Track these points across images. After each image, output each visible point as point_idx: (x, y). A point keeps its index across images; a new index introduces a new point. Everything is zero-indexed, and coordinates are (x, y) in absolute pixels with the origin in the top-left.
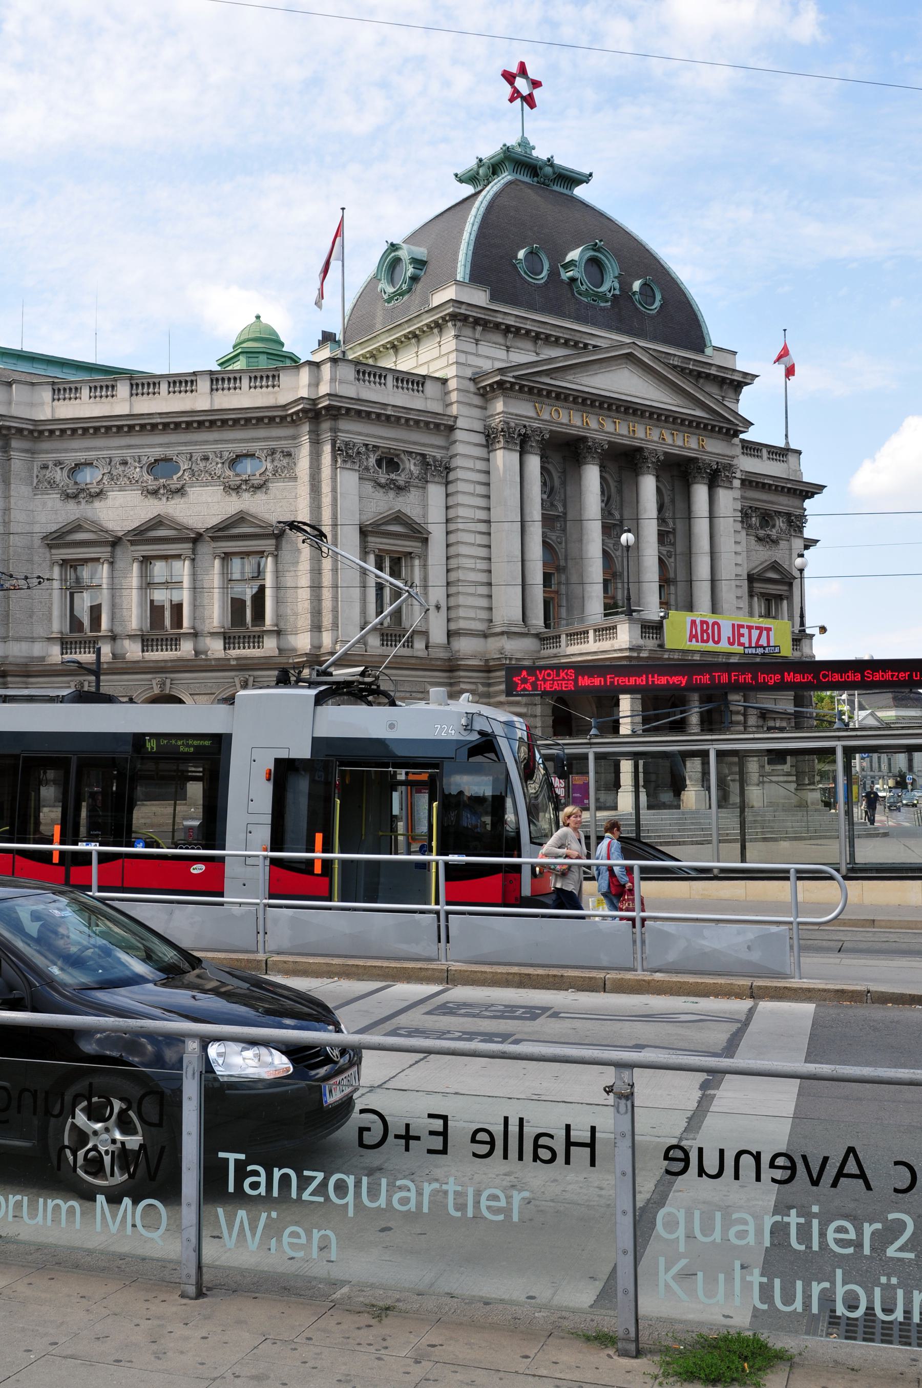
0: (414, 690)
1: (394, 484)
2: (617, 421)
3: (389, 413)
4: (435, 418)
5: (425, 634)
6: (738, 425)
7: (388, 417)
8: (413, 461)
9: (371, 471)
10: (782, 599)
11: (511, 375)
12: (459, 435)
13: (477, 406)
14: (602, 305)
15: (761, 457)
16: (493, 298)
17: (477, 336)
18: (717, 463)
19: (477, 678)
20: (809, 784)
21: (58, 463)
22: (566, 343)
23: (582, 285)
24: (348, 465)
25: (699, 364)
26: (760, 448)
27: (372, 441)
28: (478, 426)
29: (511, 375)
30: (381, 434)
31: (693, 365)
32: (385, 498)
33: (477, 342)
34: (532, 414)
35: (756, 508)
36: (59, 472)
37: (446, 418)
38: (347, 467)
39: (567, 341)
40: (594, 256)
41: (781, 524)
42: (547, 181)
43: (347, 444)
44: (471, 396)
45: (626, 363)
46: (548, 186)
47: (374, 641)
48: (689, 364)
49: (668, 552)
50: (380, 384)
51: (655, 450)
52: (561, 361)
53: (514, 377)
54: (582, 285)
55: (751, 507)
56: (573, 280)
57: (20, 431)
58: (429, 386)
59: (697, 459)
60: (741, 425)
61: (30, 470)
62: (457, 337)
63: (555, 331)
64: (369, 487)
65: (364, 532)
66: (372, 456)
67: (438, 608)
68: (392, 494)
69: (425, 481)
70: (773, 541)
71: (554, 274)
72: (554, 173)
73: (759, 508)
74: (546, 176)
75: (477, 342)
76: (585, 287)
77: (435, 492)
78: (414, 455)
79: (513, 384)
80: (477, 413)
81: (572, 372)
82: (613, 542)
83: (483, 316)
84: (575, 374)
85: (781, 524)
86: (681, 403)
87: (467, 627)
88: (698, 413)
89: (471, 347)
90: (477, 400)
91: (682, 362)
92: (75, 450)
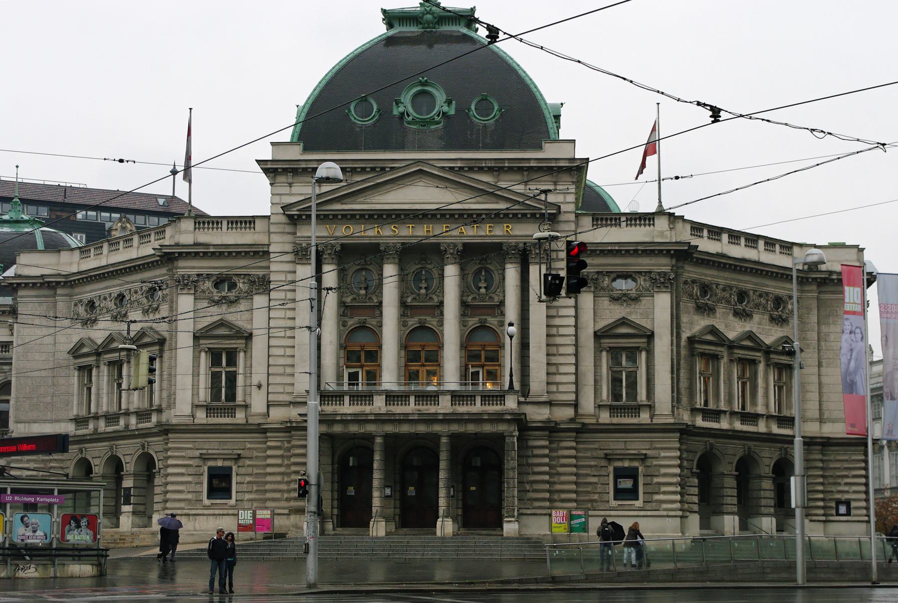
0: (235, 448)
1: (225, 299)
2: (411, 226)
3: (212, 250)
4: (252, 248)
5: (246, 407)
6: (541, 209)
7: (213, 253)
8: (241, 281)
9: (207, 293)
10: (641, 351)
11: (295, 209)
12: (272, 255)
13: (289, 233)
14: (433, 127)
15: (620, 225)
16: (306, 149)
17: (290, 180)
18: (525, 244)
19: (282, 437)
20: (507, 517)
21: (81, 301)
22: (373, 169)
23: (408, 116)
24: (185, 291)
25: (515, 161)
26: (618, 217)
27: (205, 272)
28: (289, 248)
29: (295, 209)
30: (219, 265)
31: (508, 163)
33: (290, 185)
35: (607, 272)
36: (80, 307)
37: (260, 246)
38: (184, 292)
39: (373, 169)
40: (421, 90)
41: (642, 283)
42: (431, 25)
43: (183, 276)
44: (282, 226)
45: (421, 178)
46: (434, 28)
47: (201, 417)
48: (504, 163)
49: (499, 321)
50: (217, 228)
51: (452, 243)
52: (343, 191)
53: (297, 210)
55: (598, 273)
56: (403, 114)
57: (58, 283)
58: (259, 224)
59: (501, 244)
61: (69, 307)
62: (271, 184)
63: (358, 164)
65: (196, 338)
66: (207, 282)
67: (259, 386)
68: (224, 307)
69: (249, 296)
71: (385, 113)
72: (435, 18)
73: (611, 272)
74: (428, 22)
75: (290, 185)
77: (260, 300)
78: (242, 276)
79: (300, 216)
80: (289, 238)
81: (364, 195)
82: (437, 320)
83: (288, 166)
84: (365, 196)
85: (642, 283)
87: (276, 400)
88: (502, 206)
89: (286, 190)
90: (289, 229)
91: (495, 163)
92: (87, 293)
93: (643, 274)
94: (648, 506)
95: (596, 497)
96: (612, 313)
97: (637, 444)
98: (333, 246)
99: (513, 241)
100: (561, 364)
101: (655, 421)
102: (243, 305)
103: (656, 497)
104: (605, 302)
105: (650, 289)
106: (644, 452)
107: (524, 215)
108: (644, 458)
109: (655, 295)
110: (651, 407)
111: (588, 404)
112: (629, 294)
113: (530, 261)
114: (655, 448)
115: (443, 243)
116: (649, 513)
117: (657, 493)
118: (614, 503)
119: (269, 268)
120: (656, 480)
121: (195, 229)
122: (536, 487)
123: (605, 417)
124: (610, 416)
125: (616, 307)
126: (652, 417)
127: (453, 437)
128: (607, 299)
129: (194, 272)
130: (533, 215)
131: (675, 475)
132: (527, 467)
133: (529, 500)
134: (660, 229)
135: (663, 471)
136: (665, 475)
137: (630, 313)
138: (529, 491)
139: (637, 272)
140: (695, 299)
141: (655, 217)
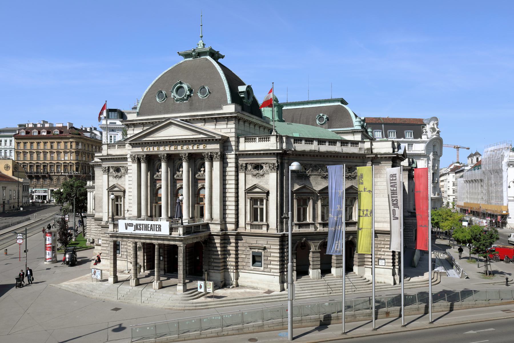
6: (215, 137)
18: (211, 152)
24: (105, 173)
26: (255, 137)
27: (110, 165)
32: (116, 180)
34: (141, 150)
35: (250, 163)
53: (129, 141)
54: (175, 97)
60: (216, 136)
64: (111, 178)
68: (118, 179)
70: (262, 176)
76: (176, 98)
86: (191, 134)
93: (265, 164)
94: (266, 270)
95: (245, 264)
96: (252, 181)
97: (262, 242)
98: (143, 156)
99: (206, 151)
100: (229, 205)
101: (269, 232)
102: (123, 179)
103: (269, 266)
104: (249, 177)
105: (268, 171)
106: (265, 245)
107: (209, 140)
108: (265, 248)
109: (270, 173)
110: (268, 226)
111: (242, 223)
112: (259, 173)
113: (214, 160)
114: (269, 244)
115: (181, 153)
116: (266, 273)
117: (270, 264)
118: (252, 267)
119: (127, 164)
120: (269, 258)
121: (108, 148)
122: (215, 261)
123: (248, 229)
124: (251, 228)
125: (255, 179)
126: (267, 230)
127: (159, 245)
128: (251, 175)
129: (107, 166)
130: (213, 140)
131: (277, 257)
132: (212, 252)
133: (213, 266)
134: (272, 143)
135: (272, 255)
136: (273, 256)
137: (260, 182)
138: (213, 262)
139: (263, 163)
140: (297, 173)
141: (271, 137)
